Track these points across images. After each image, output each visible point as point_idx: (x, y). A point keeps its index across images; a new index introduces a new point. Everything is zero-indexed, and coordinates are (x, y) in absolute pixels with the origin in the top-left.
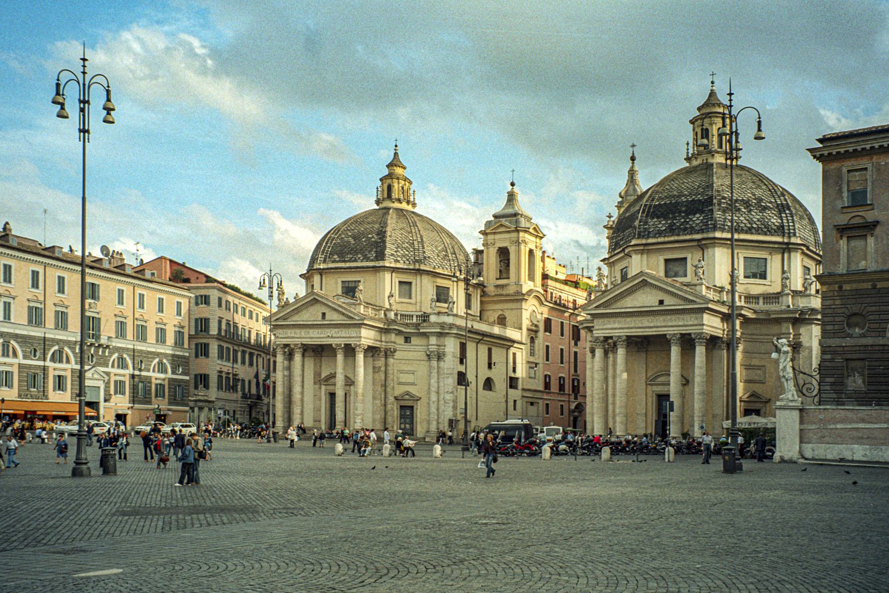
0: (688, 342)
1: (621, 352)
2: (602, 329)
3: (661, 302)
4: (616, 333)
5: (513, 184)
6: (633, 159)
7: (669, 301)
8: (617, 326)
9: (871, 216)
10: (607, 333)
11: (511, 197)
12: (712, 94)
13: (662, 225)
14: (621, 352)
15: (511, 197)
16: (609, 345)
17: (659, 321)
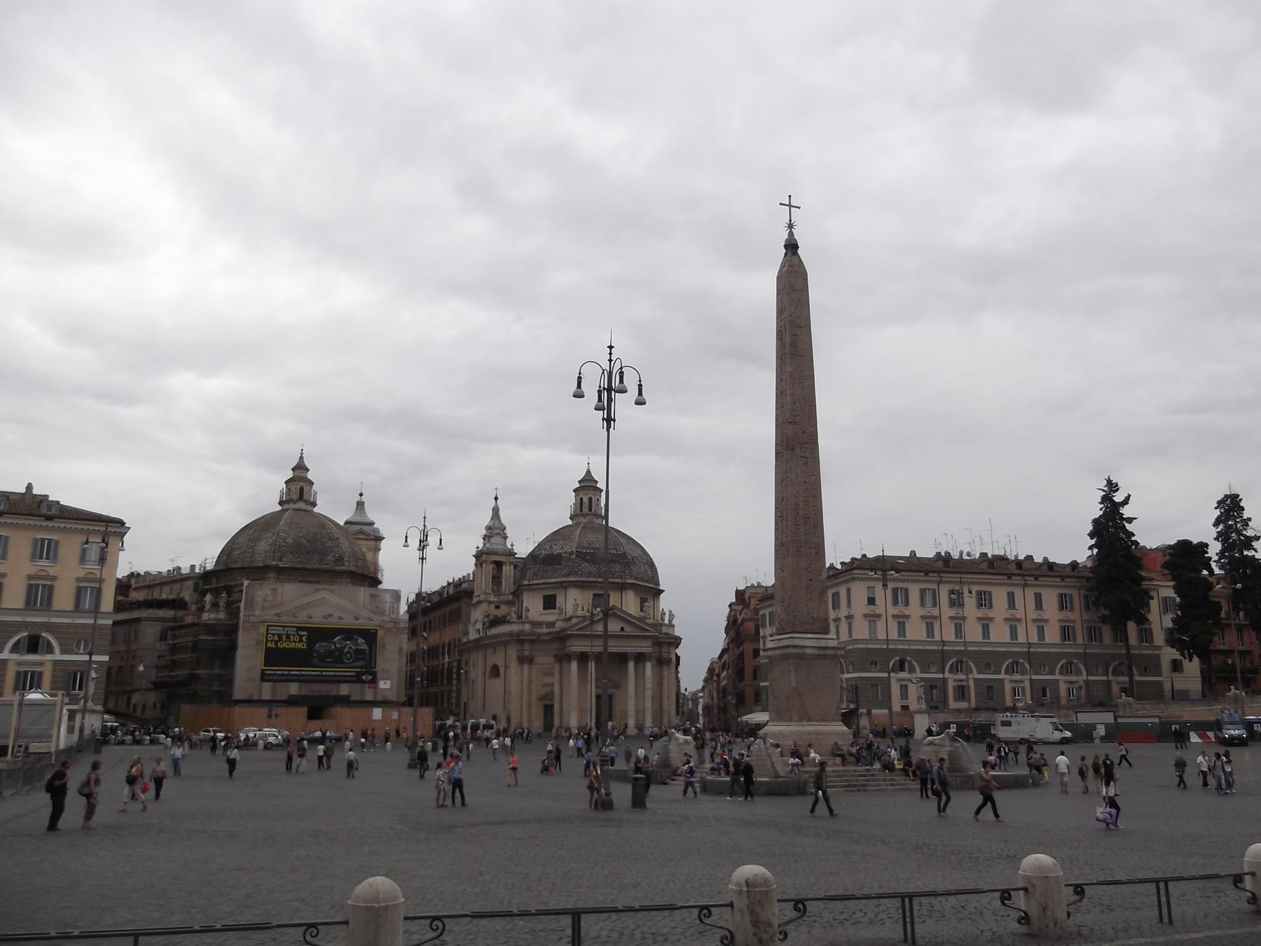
0: (640, 658)
1: (592, 666)
2: (577, 647)
3: (622, 629)
4: (588, 649)
5: (361, 495)
6: (496, 499)
7: (628, 629)
9: (878, 612)
10: (583, 649)
11: (360, 505)
12: (588, 472)
13: (592, 568)
14: (592, 666)
15: (360, 505)
16: (583, 658)
17: (622, 643)
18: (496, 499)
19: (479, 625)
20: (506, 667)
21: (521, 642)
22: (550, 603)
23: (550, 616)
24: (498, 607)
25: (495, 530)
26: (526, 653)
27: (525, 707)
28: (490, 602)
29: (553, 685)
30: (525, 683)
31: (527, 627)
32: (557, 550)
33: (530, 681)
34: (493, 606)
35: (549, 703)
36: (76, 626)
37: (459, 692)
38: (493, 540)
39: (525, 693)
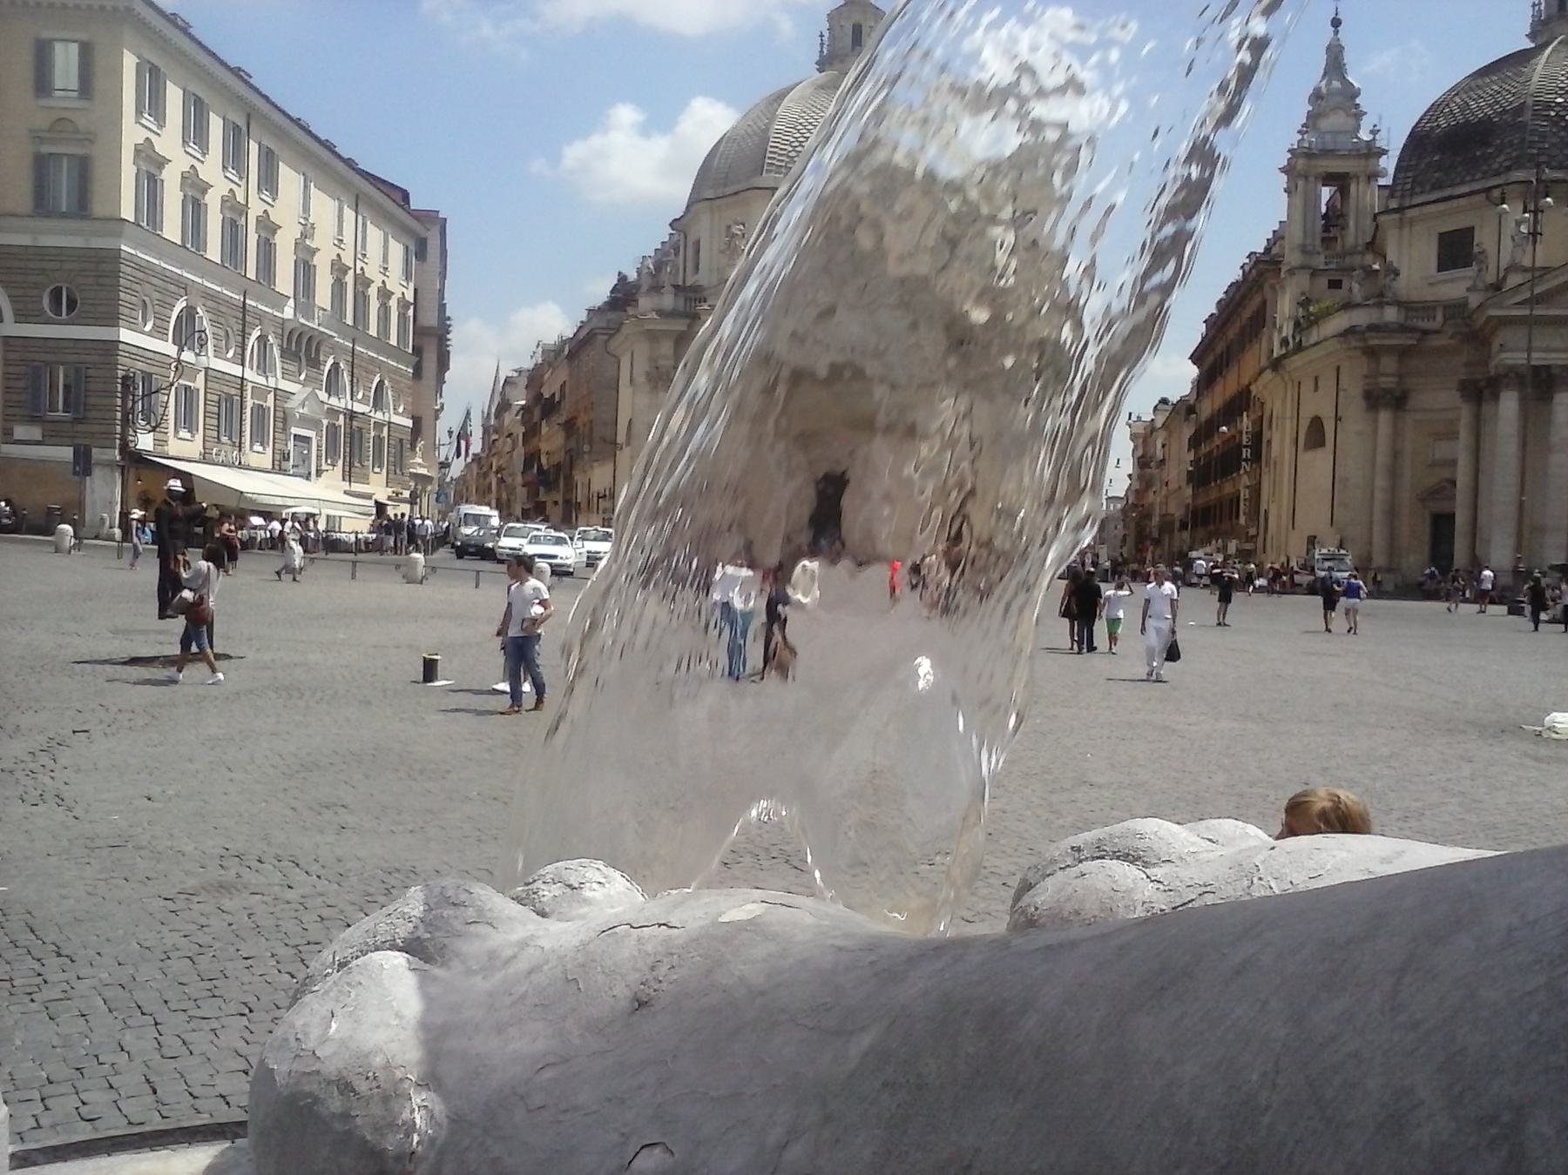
6: (1336, 23)
8: (1558, 343)
18: (1336, 23)
19: (1287, 330)
20: (1337, 419)
21: (1372, 353)
22: (1456, 250)
23: (1456, 286)
24: (1335, 284)
25: (1336, 97)
26: (1387, 382)
27: (1378, 516)
28: (1315, 273)
29: (1453, 463)
30: (1382, 458)
31: (1391, 314)
32: (1480, 107)
33: (1396, 454)
34: (1323, 282)
35: (1442, 507)
36: (41, 253)
37: (1256, 491)
38: (1324, 124)
39: (1381, 482)
